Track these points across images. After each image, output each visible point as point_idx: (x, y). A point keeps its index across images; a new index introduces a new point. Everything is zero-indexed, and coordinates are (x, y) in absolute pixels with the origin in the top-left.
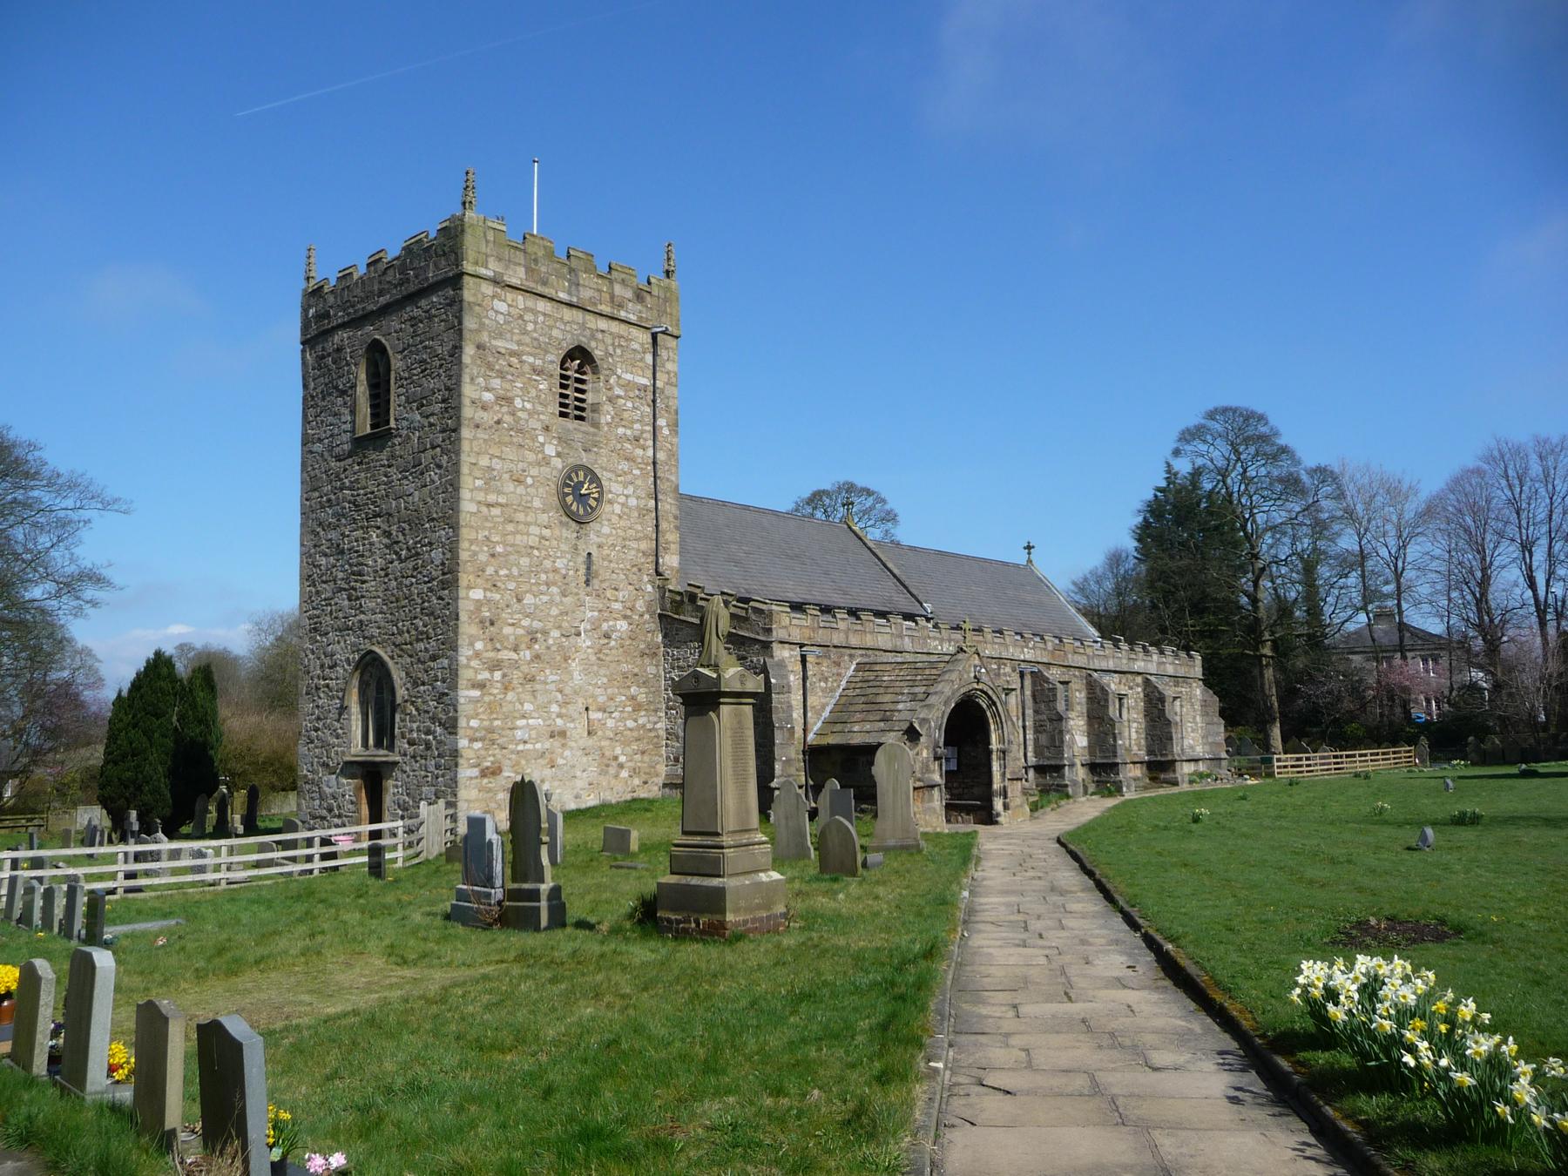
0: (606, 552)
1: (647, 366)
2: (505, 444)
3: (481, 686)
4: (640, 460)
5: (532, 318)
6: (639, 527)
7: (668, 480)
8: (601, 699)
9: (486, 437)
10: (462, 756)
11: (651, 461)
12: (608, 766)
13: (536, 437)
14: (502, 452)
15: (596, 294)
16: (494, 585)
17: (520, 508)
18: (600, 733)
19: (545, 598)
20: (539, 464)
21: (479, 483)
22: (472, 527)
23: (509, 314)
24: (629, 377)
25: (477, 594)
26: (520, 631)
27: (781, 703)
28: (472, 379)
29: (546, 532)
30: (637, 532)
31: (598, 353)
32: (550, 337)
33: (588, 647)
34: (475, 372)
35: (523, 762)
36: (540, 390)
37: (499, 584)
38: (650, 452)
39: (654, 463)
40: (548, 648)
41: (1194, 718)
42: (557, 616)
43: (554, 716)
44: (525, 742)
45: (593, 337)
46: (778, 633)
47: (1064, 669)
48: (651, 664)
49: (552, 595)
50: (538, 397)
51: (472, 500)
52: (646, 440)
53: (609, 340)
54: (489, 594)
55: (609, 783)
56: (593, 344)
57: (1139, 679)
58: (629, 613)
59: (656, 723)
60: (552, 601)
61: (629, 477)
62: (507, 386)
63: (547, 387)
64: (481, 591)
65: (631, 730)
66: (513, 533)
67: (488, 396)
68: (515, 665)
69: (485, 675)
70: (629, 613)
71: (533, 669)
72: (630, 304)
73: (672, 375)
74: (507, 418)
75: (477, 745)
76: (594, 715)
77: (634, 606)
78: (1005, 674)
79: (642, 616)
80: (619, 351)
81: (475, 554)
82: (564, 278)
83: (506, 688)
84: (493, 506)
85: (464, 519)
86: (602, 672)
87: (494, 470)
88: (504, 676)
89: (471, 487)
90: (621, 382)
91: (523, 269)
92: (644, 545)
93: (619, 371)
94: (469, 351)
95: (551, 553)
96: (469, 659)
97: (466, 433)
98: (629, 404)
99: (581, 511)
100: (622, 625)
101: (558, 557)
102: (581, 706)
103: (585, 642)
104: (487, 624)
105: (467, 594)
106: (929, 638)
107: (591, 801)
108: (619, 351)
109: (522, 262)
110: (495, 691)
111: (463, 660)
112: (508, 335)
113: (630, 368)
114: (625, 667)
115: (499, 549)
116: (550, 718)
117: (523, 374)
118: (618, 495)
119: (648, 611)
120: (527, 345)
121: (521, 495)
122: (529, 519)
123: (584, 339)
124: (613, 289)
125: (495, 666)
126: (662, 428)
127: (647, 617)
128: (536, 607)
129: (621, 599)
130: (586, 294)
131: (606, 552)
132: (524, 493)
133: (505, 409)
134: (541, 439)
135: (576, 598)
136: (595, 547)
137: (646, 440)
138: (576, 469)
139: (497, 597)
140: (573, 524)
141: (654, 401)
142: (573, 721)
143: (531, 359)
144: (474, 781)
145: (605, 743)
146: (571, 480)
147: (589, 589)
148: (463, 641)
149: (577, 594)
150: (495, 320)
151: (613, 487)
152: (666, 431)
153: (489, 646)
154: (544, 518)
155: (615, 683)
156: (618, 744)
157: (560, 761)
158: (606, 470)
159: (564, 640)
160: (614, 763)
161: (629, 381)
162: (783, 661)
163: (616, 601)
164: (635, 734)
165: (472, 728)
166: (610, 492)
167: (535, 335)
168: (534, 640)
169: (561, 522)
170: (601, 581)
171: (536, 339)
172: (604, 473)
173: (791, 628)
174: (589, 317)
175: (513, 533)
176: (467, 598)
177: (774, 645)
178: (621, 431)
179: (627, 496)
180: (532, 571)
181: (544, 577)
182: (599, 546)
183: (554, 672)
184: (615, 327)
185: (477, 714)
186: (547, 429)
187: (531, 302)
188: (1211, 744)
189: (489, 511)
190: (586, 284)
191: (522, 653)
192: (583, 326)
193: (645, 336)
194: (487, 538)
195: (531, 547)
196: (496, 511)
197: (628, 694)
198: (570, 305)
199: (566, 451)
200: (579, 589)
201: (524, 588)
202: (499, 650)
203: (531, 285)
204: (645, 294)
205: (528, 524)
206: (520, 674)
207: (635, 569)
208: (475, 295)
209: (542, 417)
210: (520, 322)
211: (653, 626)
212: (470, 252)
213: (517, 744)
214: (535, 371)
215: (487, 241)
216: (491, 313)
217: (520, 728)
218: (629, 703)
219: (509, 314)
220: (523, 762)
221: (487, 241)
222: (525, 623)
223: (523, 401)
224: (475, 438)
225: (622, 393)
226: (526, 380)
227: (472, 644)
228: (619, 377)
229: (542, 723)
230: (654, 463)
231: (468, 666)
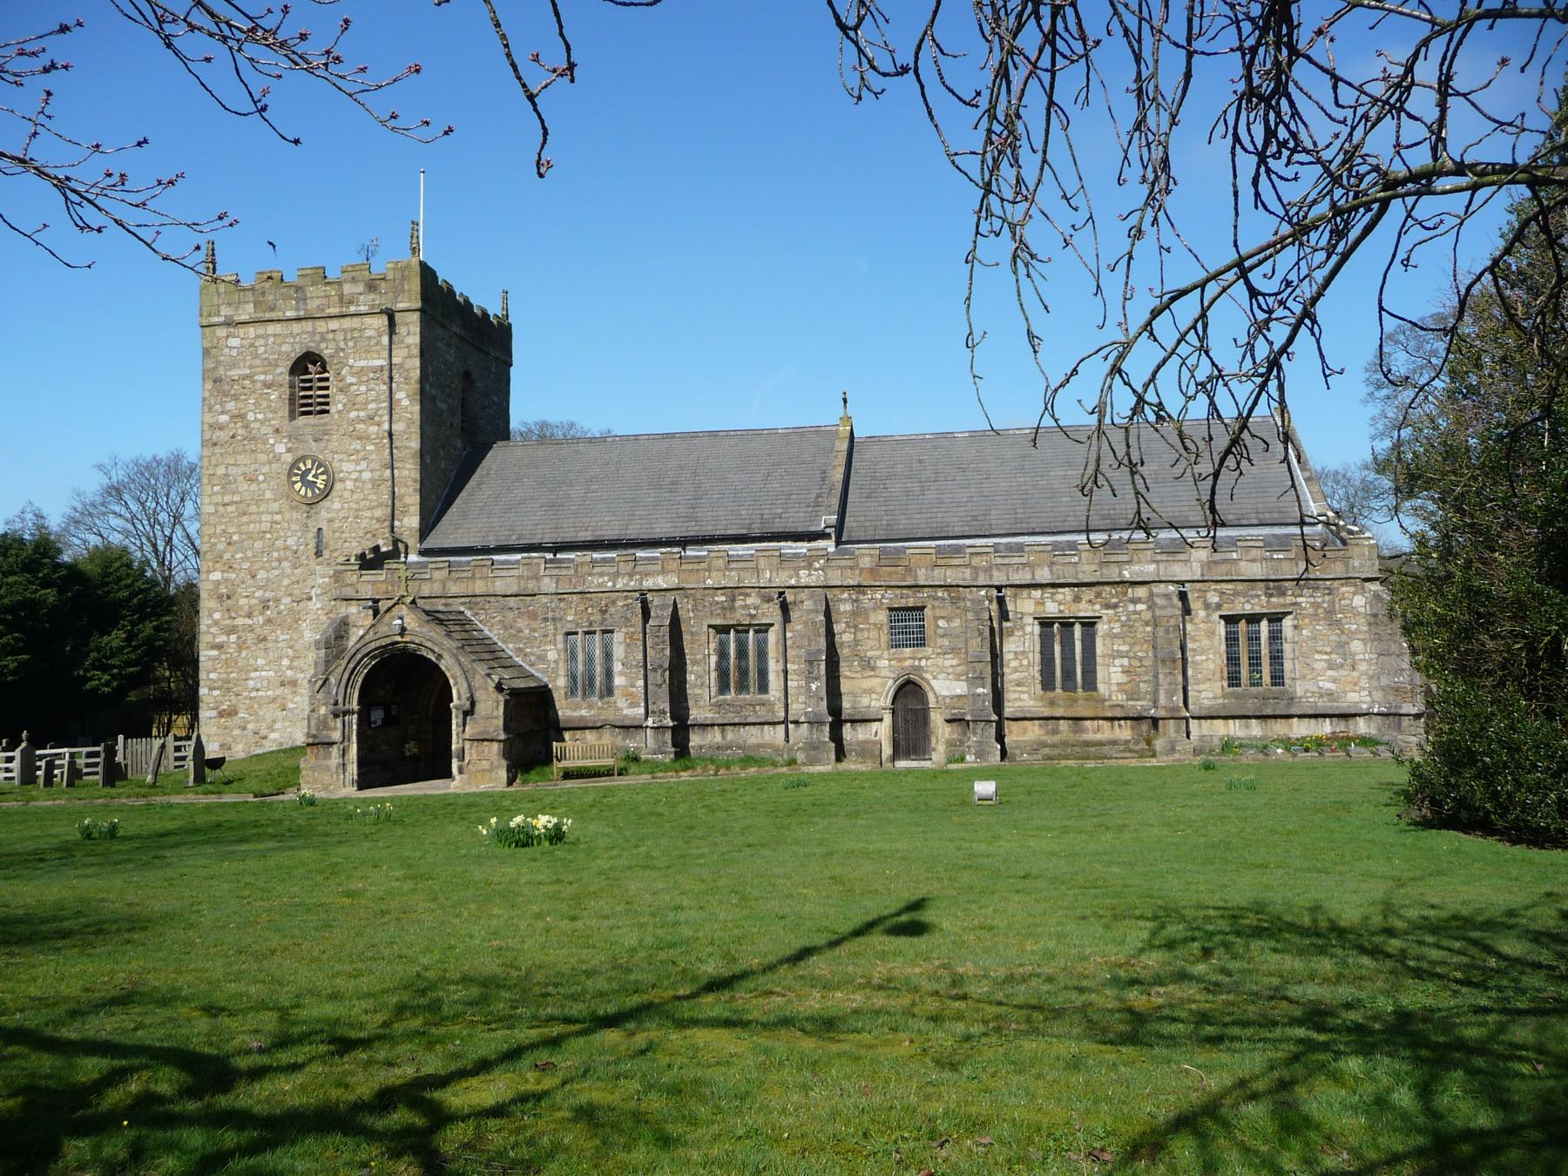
0: (337, 524)
3: (220, 647)
6: (374, 497)
7: (406, 447)
13: (265, 442)
15: (324, 301)
19: (276, 572)
20: (270, 463)
24: (363, 363)
25: (216, 576)
26: (254, 601)
29: (278, 518)
30: (372, 501)
35: (256, 706)
38: (386, 426)
39: (391, 435)
40: (279, 613)
41: (1341, 647)
45: (323, 339)
47: (898, 591)
50: (269, 407)
51: (210, 503)
53: (340, 336)
54: (226, 575)
57: (1141, 592)
60: (282, 575)
62: (240, 405)
66: (248, 523)
67: (224, 418)
69: (224, 638)
71: (267, 630)
72: (362, 297)
74: (240, 431)
75: (216, 693)
78: (747, 607)
80: (351, 344)
83: (240, 649)
88: (239, 638)
90: (354, 370)
92: (379, 513)
96: (209, 627)
98: (363, 388)
103: (315, 605)
106: (591, 575)
108: (351, 344)
115: (235, 538)
117: (254, 392)
118: (350, 473)
123: (313, 345)
125: (231, 630)
126: (400, 400)
130: (312, 305)
131: (337, 524)
133: (239, 424)
134: (272, 441)
138: (303, 459)
143: (262, 377)
146: (299, 469)
147: (320, 559)
151: (346, 468)
153: (226, 616)
154: (276, 506)
157: (291, 706)
167: (266, 356)
168: (266, 607)
174: (318, 323)
175: (248, 523)
178: (353, 415)
179: (360, 472)
181: (275, 555)
182: (330, 521)
184: (347, 323)
186: (277, 431)
187: (261, 330)
188: (1383, 689)
194: (224, 531)
195: (264, 532)
196: (230, 509)
198: (298, 319)
201: (258, 565)
205: (259, 513)
207: (369, 536)
216: (226, 351)
224: (213, 454)
225: (354, 380)
227: (210, 615)
228: (351, 367)
230: (391, 435)
231: (209, 632)
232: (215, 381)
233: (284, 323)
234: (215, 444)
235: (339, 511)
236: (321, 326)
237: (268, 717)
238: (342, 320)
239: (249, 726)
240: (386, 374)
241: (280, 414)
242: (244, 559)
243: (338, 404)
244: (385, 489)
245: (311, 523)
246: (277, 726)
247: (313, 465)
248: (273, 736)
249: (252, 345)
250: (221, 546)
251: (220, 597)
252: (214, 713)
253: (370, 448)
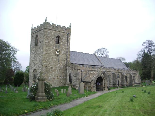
3: (45, 73)
13: (52, 46)
19: (53, 64)
20: (53, 49)
24: (64, 39)
25: (45, 63)
29: (53, 56)
54: (46, 63)
63: (54, 40)
67: (47, 42)
68: (49, 71)
69: (46, 72)
71: (51, 71)
74: (49, 44)
100: (62, 67)
103: (58, 68)
107: (58, 86)
115: (48, 58)
125: (47, 71)
134: (53, 46)
145: (60, 80)
152: (69, 45)
168: (51, 68)
182: (60, 58)
186: (54, 45)
196: (47, 54)
205: (51, 56)
214: (53, 39)
227: (44, 69)
242: (49, 61)
244: (66, 55)
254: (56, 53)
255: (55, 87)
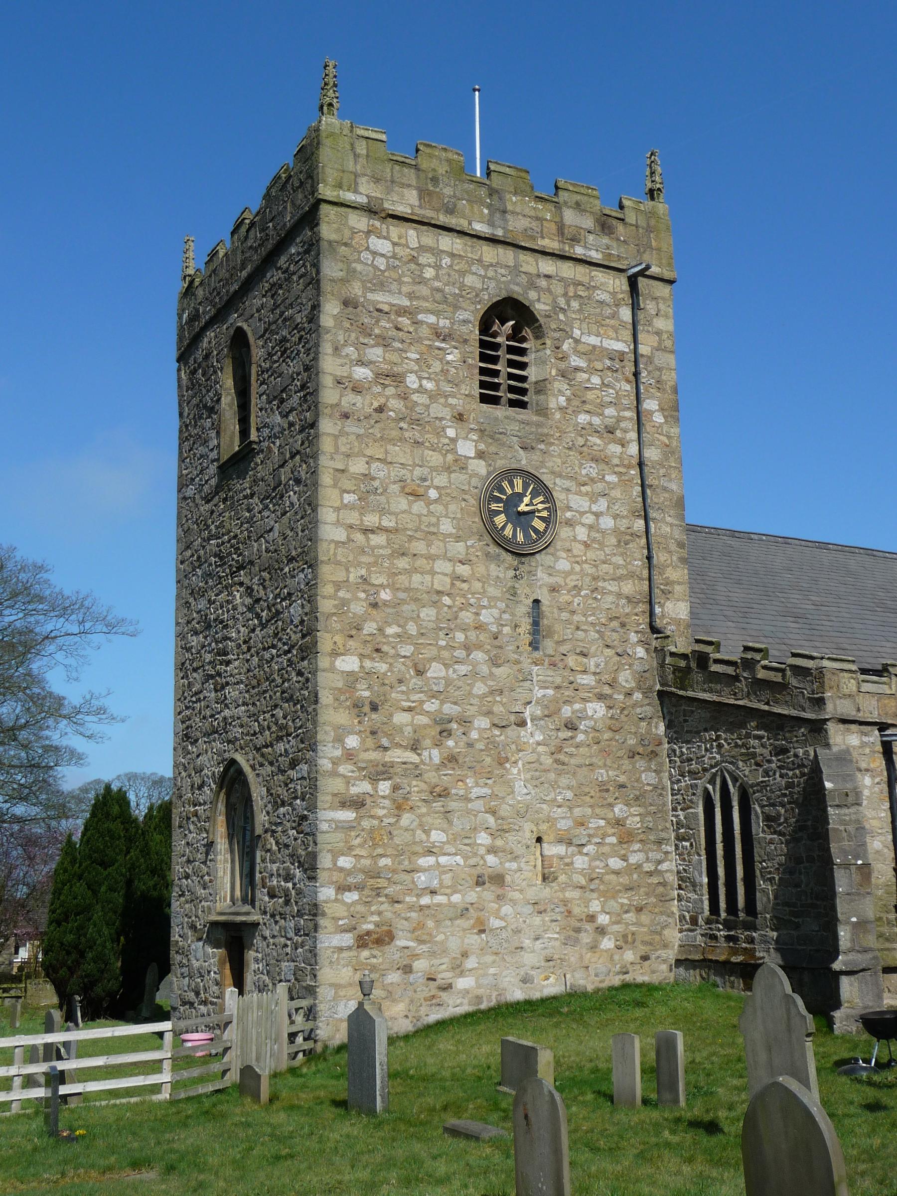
0: (564, 597)
1: (623, 324)
2: (391, 441)
3: (357, 804)
4: (616, 461)
5: (432, 260)
6: (619, 560)
7: (665, 489)
8: (563, 825)
9: (362, 431)
10: (324, 914)
11: (635, 461)
12: (578, 930)
14: (386, 452)
15: (535, 225)
16: (378, 650)
17: (418, 535)
18: (562, 878)
19: (463, 669)
20: (448, 469)
21: (348, 498)
22: (339, 563)
23: (394, 256)
24: (593, 340)
26: (423, 720)
27: (843, 822)
28: (336, 349)
29: (463, 570)
31: (540, 308)
32: (462, 287)
33: (538, 744)
34: (341, 338)
35: (430, 924)
36: (448, 362)
37: (385, 648)
38: (633, 449)
39: (641, 464)
40: (470, 745)
42: (484, 696)
43: (482, 851)
44: (433, 892)
45: (532, 285)
46: (835, 706)
48: (649, 769)
49: (475, 665)
50: (444, 372)
51: (338, 523)
52: (625, 431)
53: (558, 289)
54: (368, 664)
55: (581, 957)
56: (533, 295)
58: (607, 690)
59: (660, 862)
60: (474, 674)
61: (599, 486)
62: (394, 357)
64: (356, 659)
65: (617, 873)
68: (416, 771)
69: (365, 787)
70: (607, 690)
71: (446, 777)
72: (591, 238)
73: (665, 336)
74: (394, 403)
75: (351, 897)
76: (553, 850)
77: (615, 680)
79: (629, 694)
80: (575, 304)
81: (344, 603)
82: (482, 203)
83: (399, 808)
84: (372, 531)
85: (324, 551)
86: (564, 781)
87: (374, 479)
88: (396, 788)
89: (337, 504)
90: (580, 348)
91: (415, 192)
92: (628, 588)
93: (577, 333)
94: (330, 310)
95: (472, 601)
96: (335, 762)
97: (327, 426)
98: (596, 380)
99: (520, 537)
100: (597, 710)
101: (484, 607)
102: (528, 831)
103: (532, 735)
104: (367, 709)
105: (332, 664)
107: (551, 987)
108: (575, 304)
109: (414, 183)
110: (381, 812)
111: (325, 764)
112: (394, 287)
113: (594, 328)
114: (602, 774)
116: (475, 854)
117: (419, 340)
118: (582, 514)
119: (639, 688)
120: (425, 299)
121: (419, 516)
122: (433, 550)
123: (516, 288)
124: (562, 218)
126: (651, 413)
127: (637, 696)
128: (448, 682)
129: (593, 669)
130: (517, 225)
131: (564, 597)
132: (425, 512)
133: (390, 391)
134: (451, 433)
135: (516, 667)
136: (545, 590)
137: (625, 431)
138: (510, 474)
139: (383, 667)
140: (509, 558)
141: (636, 374)
142: (515, 858)
143: (432, 319)
144: (345, 954)
145: (569, 894)
146: (502, 490)
147: (537, 655)
148: (325, 734)
149: (518, 662)
150: (372, 265)
152: (659, 418)
153: (370, 743)
155: (587, 799)
156: (595, 895)
157: (495, 923)
158: (560, 476)
159: (497, 732)
160: (589, 927)
161: (594, 347)
162: (847, 751)
163: (585, 672)
164: (624, 880)
165: (341, 870)
166: (569, 508)
167: (437, 284)
168: (444, 733)
169: (487, 555)
170: (558, 643)
171: (438, 290)
172: (558, 480)
173: (860, 699)
174: (524, 257)
175: (409, 572)
176: (332, 669)
177: (831, 727)
178: (583, 418)
179: (597, 515)
180: (441, 629)
181: (460, 637)
182: (554, 589)
183: (482, 781)
184: (567, 270)
185: (351, 848)
186: (460, 418)
187: (429, 238)
189: (368, 539)
190: (518, 210)
191: (426, 753)
192: (516, 270)
193: (617, 281)
194: (365, 580)
195: (439, 592)
196: (378, 540)
197: (610, 815)
198: (493, 240)
199: (493, 449)
200: (521, 654)
201: (428, 653)
202: (386, 749)
203: (428, 214)
204: (615, 222)
205: (431, 558)
206: (423, 786)
207: (615, 624)
208: (338, 230)
209: (451, 401)
210: (413, 266)
211: (648, 710)
212: (328, 171)
213: (419, 896)
214: (438, 334)
215: (356, 156)
216: (366, 256)
217: (424, 870)
218: (611, 831)
219: (394, 256)
220: (430, 924)
221: (356, 156)
222: (431, 706)
223: (420, 378)
224: (342, 433)
225: (583, 364)
226: (424, 349)
227: (339, 740)
228: (577, 341)
229: (462, 862)
230: (641, 464)
231: (334, 774)
232: (346, 303)
233: (469, 241)
234: (346, 416)
235: (568, 574)
236: (529, 263)
237: (454, 945)
238: (560, 263)
239: (420, 965)
240: (630, 368)
241: (465, 389)
243: (557, 400)
245: (522, 588)
246: (471, 963)
247: (525, 486)
248: (463, 983)
249: (414, 259)
250: (358, 608)
251: (357, 705)
252: (348, 939)
253: (611, 478)
254: (500, 520)
255: (518, 995)
